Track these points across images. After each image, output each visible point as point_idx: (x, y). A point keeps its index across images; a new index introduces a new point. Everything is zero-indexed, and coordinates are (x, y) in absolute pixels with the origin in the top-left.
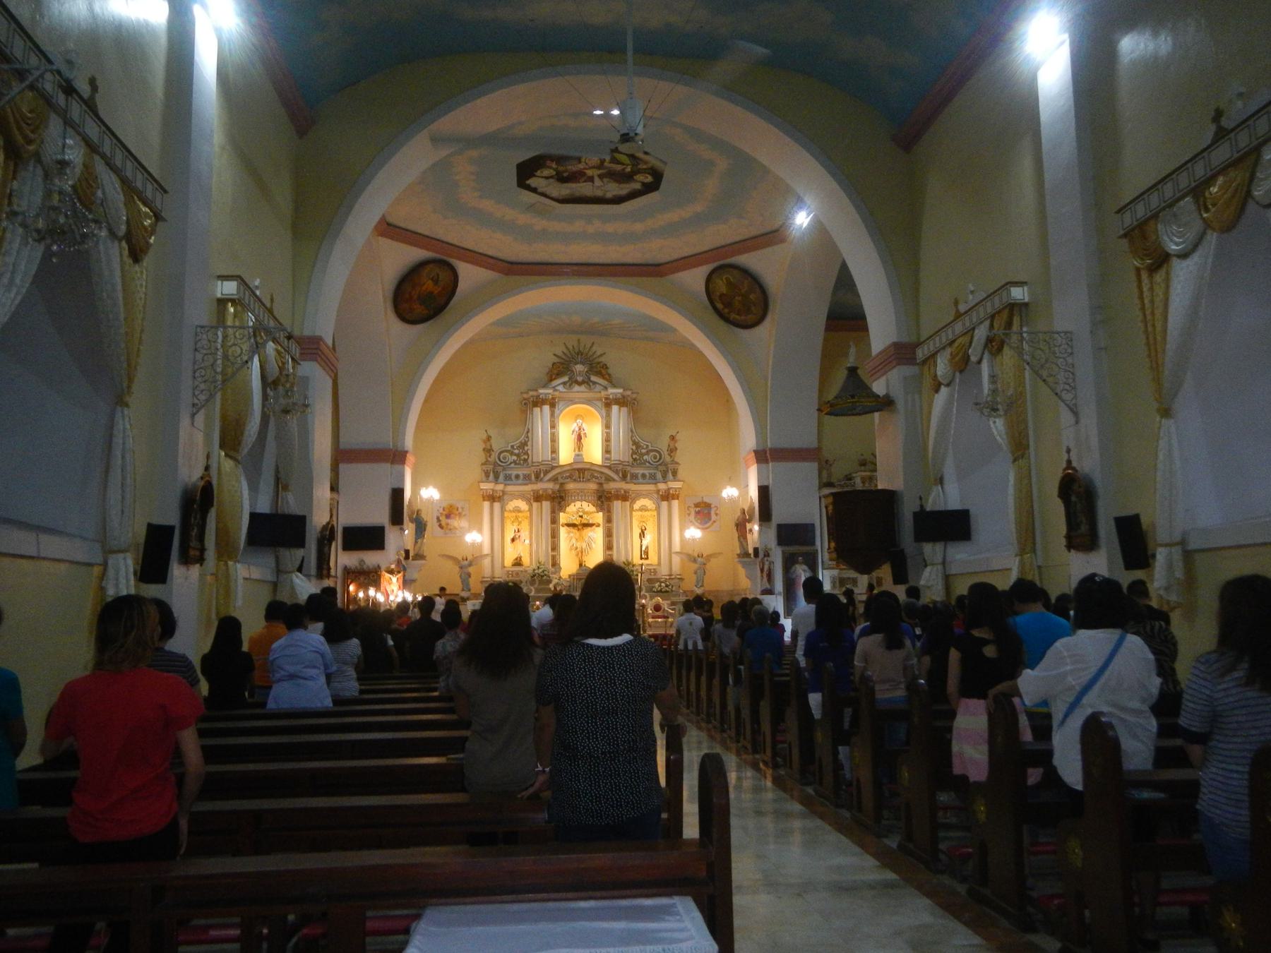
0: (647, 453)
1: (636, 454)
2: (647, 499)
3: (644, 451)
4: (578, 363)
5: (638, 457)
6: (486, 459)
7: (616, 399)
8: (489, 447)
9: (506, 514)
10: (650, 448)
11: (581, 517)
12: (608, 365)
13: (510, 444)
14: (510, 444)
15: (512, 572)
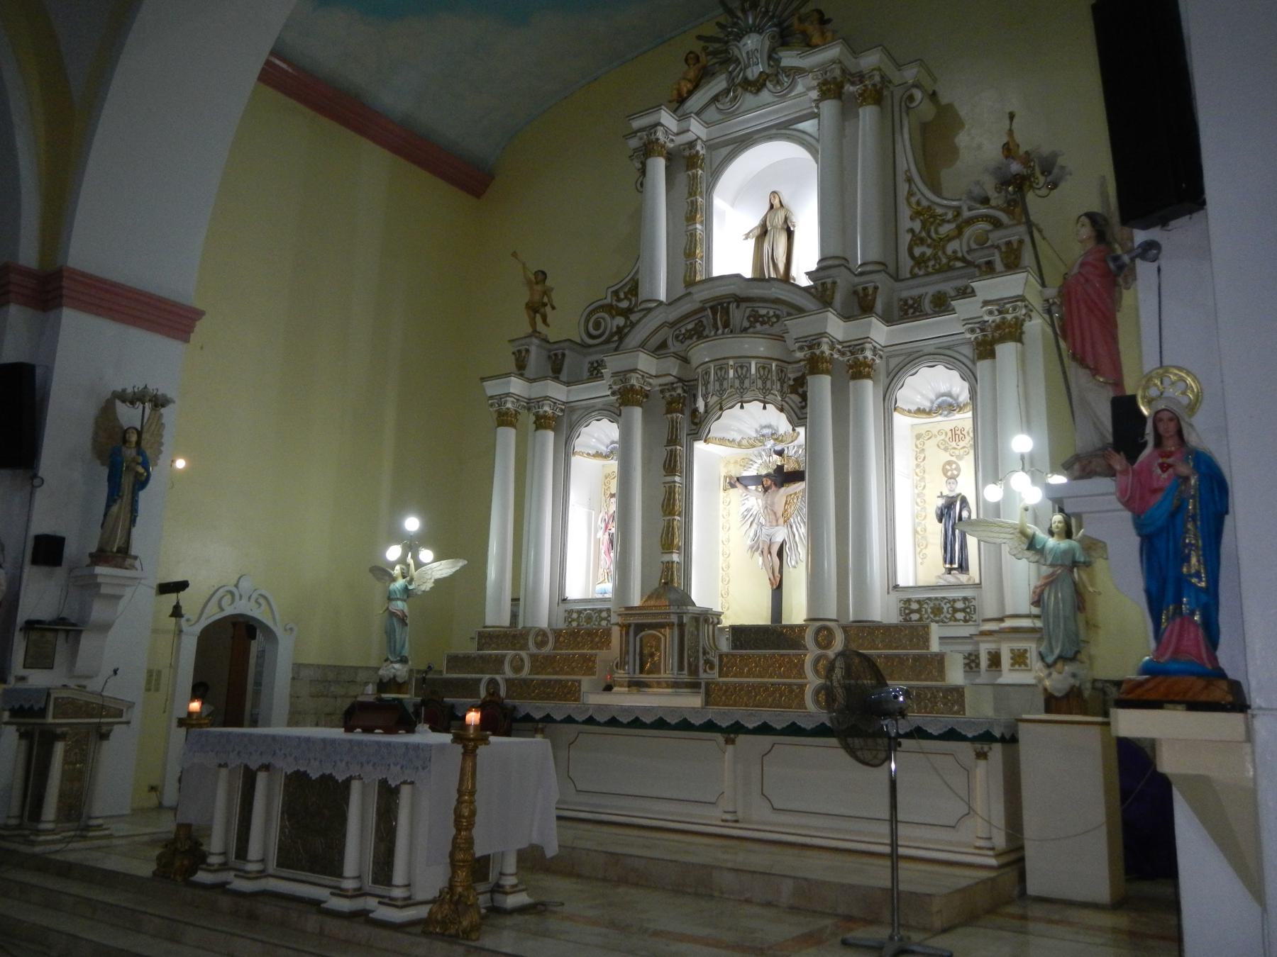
0: (960, 231)
1: (922, 241)
2: (940, 369)
3: (945, 229)
4: (744, 35)
5: (929, 252)
6: (533, 324)
7: (825, 83)
8: (537, 298)
9: (575, 460)
10: (966, 214)
11: (780, 453)
12: (826, 17)
13: (611, 290)
14: (611, 290)
15: (580, 612)
